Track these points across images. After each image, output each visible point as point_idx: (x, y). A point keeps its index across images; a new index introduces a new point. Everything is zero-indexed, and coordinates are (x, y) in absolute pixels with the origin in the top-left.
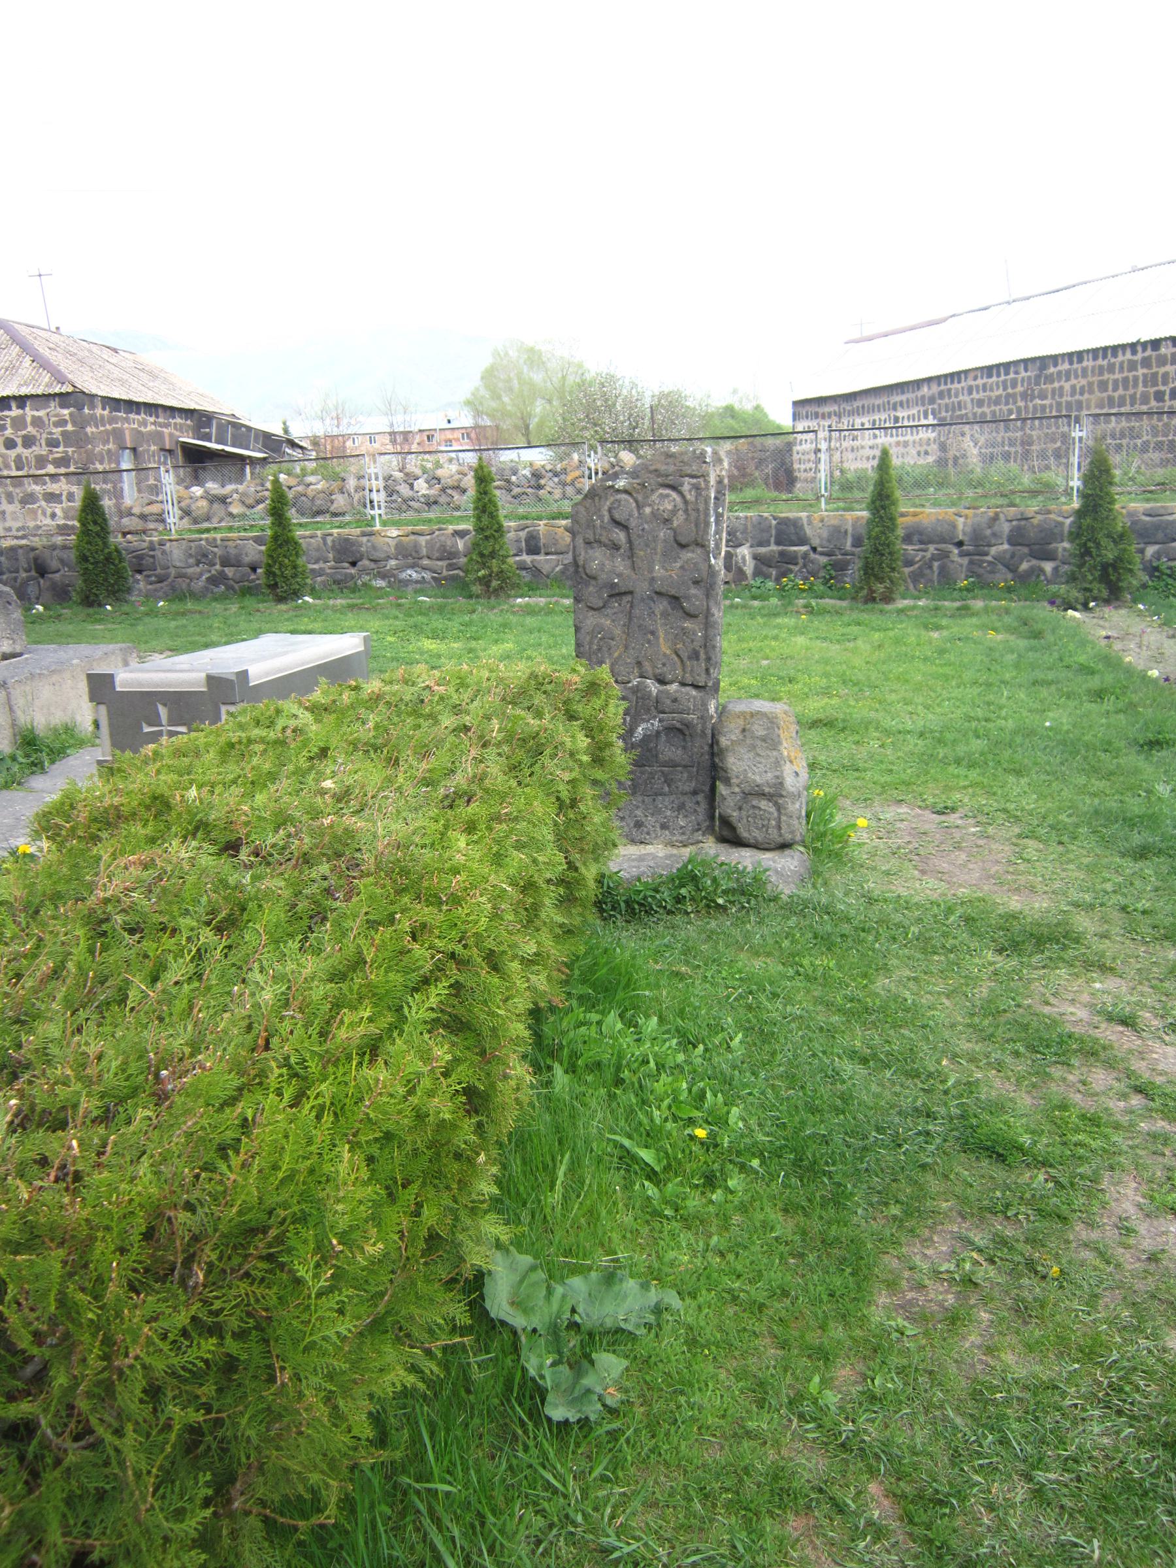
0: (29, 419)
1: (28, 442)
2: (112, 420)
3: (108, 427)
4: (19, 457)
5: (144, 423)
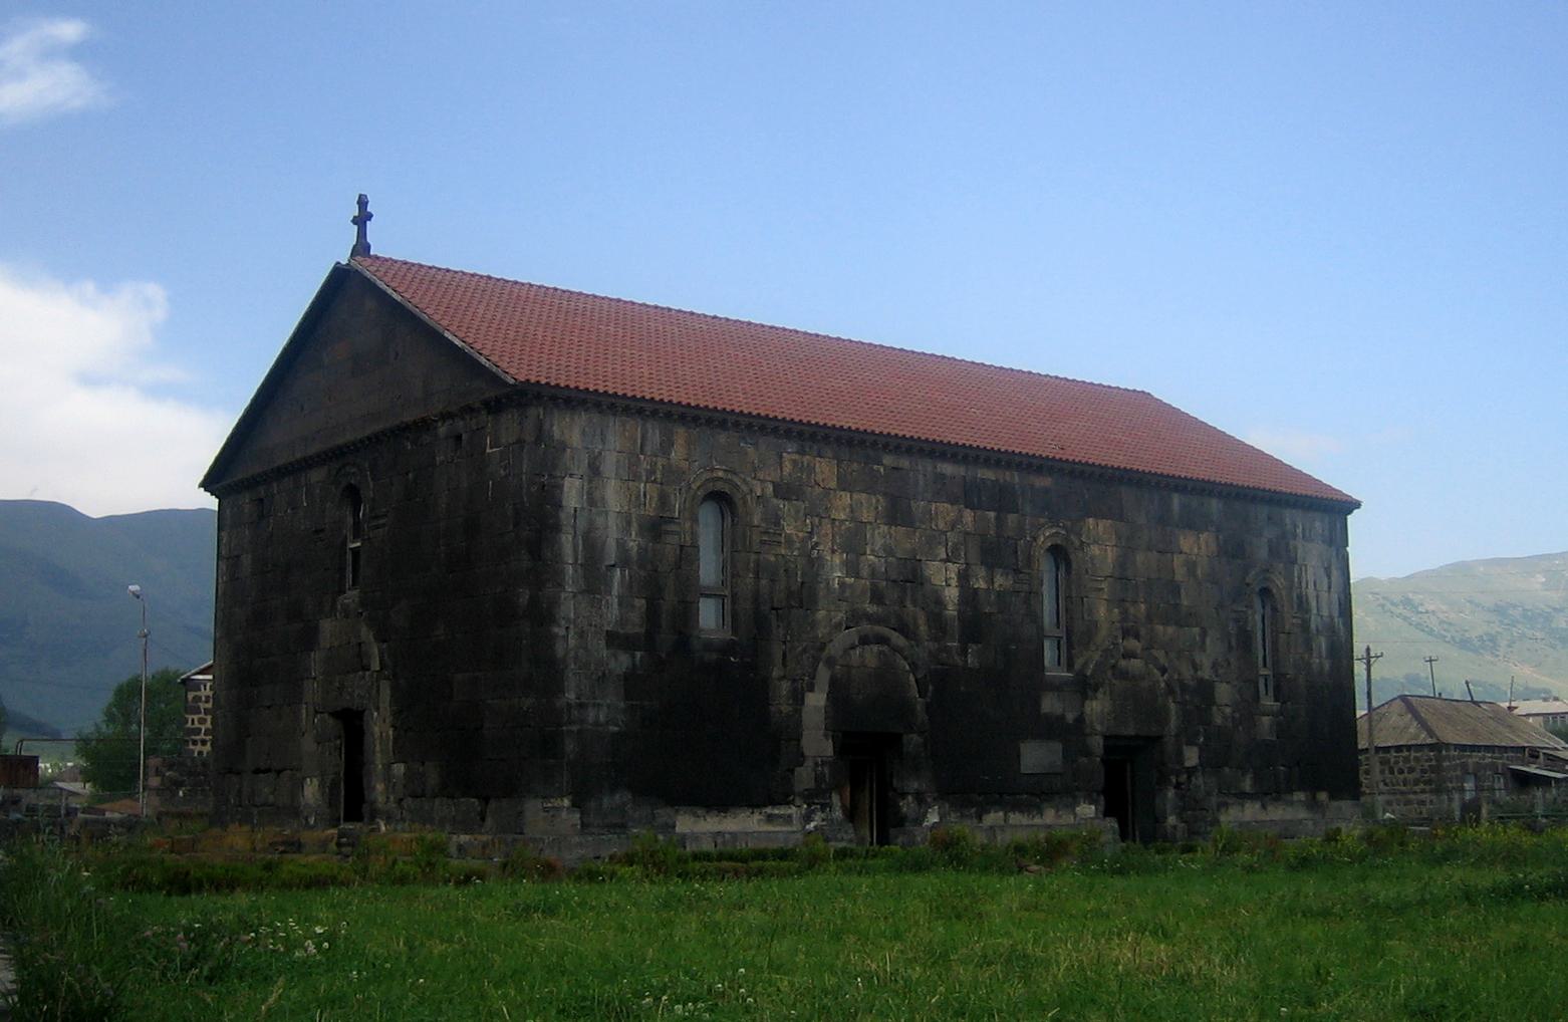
0: (1412, 757)
1: (1411, 770)
2: (1463, 757)
3: (1458, 762)
4: (1405, 779)
5: (1484, 758)
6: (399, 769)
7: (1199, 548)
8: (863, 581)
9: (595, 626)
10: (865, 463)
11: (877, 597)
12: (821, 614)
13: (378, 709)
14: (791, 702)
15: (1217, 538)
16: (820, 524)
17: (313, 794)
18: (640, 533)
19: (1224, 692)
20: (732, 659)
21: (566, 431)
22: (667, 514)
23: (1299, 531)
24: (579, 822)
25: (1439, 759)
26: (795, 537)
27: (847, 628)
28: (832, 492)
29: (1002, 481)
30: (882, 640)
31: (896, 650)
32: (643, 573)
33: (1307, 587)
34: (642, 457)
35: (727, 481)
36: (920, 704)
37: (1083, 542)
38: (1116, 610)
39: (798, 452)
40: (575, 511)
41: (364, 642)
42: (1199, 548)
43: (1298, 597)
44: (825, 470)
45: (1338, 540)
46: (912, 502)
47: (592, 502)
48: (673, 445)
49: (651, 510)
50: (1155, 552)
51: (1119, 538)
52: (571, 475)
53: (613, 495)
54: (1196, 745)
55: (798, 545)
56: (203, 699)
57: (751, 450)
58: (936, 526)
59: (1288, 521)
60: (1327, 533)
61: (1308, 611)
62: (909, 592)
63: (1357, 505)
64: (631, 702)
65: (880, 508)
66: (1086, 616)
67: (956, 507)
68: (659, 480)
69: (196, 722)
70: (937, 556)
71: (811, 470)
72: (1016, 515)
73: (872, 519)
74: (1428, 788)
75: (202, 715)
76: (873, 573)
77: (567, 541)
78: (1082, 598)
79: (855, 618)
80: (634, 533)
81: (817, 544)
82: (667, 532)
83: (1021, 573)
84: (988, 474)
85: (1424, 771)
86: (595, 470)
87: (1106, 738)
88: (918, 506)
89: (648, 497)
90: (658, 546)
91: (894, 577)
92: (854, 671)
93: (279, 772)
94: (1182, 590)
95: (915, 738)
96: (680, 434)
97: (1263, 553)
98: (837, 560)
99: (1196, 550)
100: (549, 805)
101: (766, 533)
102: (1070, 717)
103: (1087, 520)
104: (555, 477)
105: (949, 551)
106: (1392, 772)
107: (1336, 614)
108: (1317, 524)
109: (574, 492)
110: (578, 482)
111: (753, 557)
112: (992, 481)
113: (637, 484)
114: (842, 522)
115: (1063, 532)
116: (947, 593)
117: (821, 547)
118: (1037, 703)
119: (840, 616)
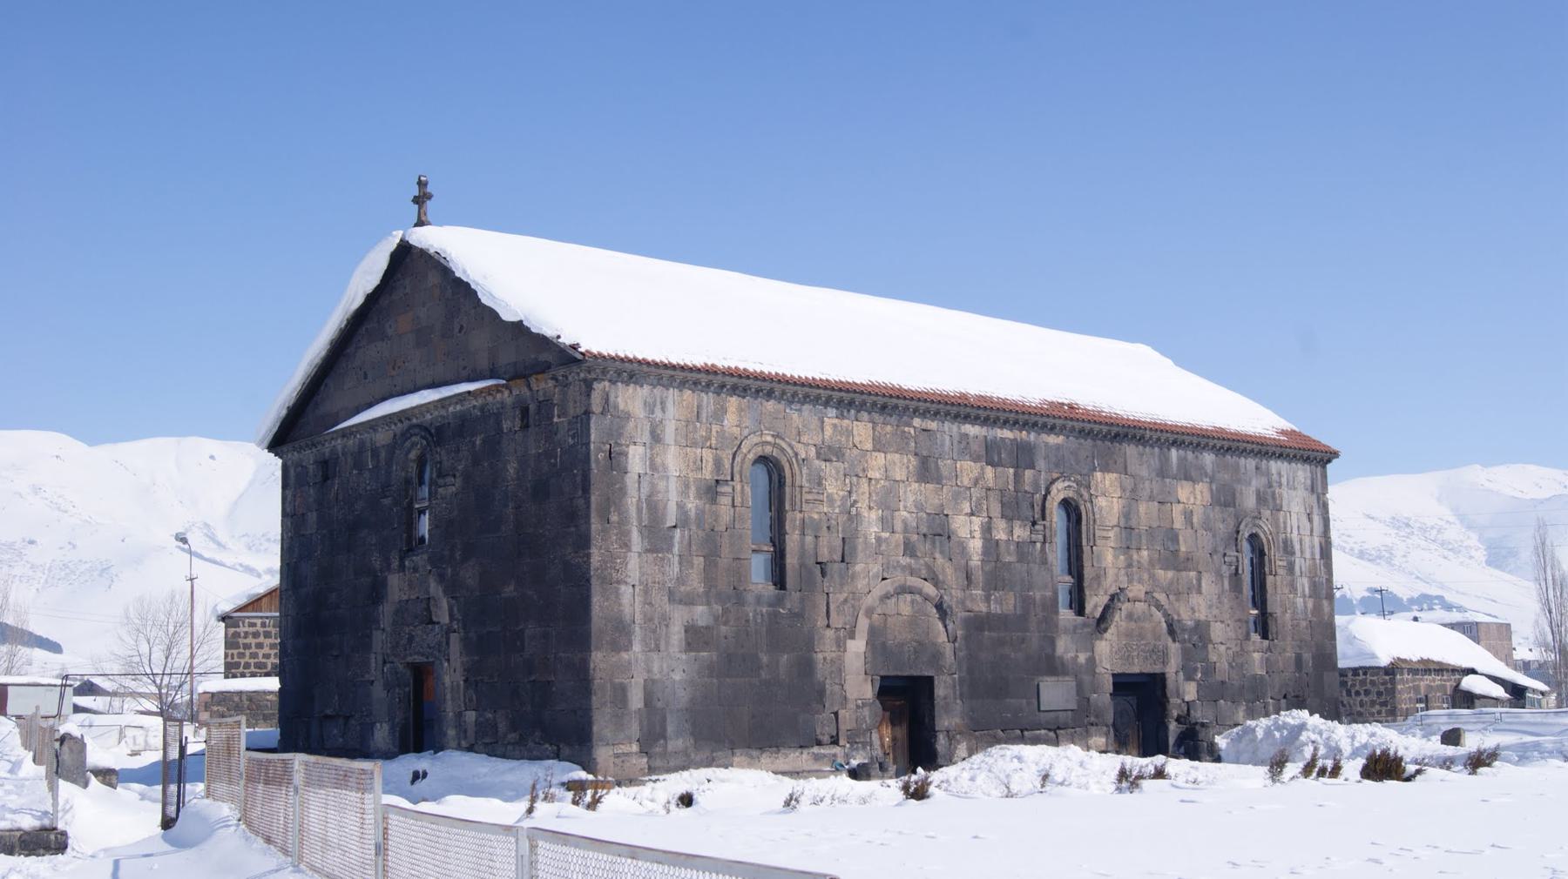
0: (1368, 681)
1: (1367, 693)
2: (1414, 681)
3: (1411, 685)
4: (1361, 700)
5: (1434, 681)
6: (471, 716)
7: (1195, 498)
9: (659, 583)
10: (897, 426)
12: (859, 567)
13: (448, 660)
15: (1211, 490)
16: (858, 483)
17: (384, 738)
19: (1218, 632)
20: (781, 610)
23: (1284, 480)
24: (647, 766)
25: (1393, 682)
26: (836, 496)
27: (883, 579)
29: (1019, 440)
30: (911, 591)
33: (1291, 532)
34: (698, 424)
35: (774, 445)
36: (948, 649)
37: (1091, 495)
38: (1122, 557)
39: (837, 417)
40: (640, 477)
41: (433, 598)
42: (1195, 498)
43: (1283, 543)
44: (862, 430)
45: (1318, 489)
47: (653, 467)
49: (708, 474)
50: (1156, 504)
51: (1123, 490)
52: (635, 443)
53: (673, 460)
54: (1194, 680)
55: (839, 503)
56: (242, 635)
57: (795, 416)
58: (961, 482)
59: (1274, 471)
60: (1309, 482)
61: (1293, 553)
62: (938, 544)
63: (1335, 454)
64: (693, 654)
65: (911, 467)
66: (1095, 564)
68: (713, 446)
69: (235, 657)
70: (962, 510)
71: (849, 433)
72: (1032, 471)
74: (1384, 709)
75: (241, 650)
76: (906, 530)
77: (631, 502)
78: (1092, 547)
81: (855, 502)
82: (723, 494)
84: (1007, 434)
85: (1379, 694)
86: (656, 438)
87: (1114, 675)
88: (945, 465)
89: (704, 461)
91: (924, 530)
92: (889, 619)
93: (347, 718)
94: (1181, 538)
96: (733, 402)
97: (1250, 501)
98: (874, 515)
99: (1192, 500)
100: (620, 751)
102: (1082, 658)
105: (973, 504)
106: (1349, 693)
107: (1318, 556)
108: (1300, 473)
109: (637, 457)
111: (799, 516)
113: (694, 449)
114: (877, 481)
115: (1075, 485)
117: (859, 505)
119: (876, 568)
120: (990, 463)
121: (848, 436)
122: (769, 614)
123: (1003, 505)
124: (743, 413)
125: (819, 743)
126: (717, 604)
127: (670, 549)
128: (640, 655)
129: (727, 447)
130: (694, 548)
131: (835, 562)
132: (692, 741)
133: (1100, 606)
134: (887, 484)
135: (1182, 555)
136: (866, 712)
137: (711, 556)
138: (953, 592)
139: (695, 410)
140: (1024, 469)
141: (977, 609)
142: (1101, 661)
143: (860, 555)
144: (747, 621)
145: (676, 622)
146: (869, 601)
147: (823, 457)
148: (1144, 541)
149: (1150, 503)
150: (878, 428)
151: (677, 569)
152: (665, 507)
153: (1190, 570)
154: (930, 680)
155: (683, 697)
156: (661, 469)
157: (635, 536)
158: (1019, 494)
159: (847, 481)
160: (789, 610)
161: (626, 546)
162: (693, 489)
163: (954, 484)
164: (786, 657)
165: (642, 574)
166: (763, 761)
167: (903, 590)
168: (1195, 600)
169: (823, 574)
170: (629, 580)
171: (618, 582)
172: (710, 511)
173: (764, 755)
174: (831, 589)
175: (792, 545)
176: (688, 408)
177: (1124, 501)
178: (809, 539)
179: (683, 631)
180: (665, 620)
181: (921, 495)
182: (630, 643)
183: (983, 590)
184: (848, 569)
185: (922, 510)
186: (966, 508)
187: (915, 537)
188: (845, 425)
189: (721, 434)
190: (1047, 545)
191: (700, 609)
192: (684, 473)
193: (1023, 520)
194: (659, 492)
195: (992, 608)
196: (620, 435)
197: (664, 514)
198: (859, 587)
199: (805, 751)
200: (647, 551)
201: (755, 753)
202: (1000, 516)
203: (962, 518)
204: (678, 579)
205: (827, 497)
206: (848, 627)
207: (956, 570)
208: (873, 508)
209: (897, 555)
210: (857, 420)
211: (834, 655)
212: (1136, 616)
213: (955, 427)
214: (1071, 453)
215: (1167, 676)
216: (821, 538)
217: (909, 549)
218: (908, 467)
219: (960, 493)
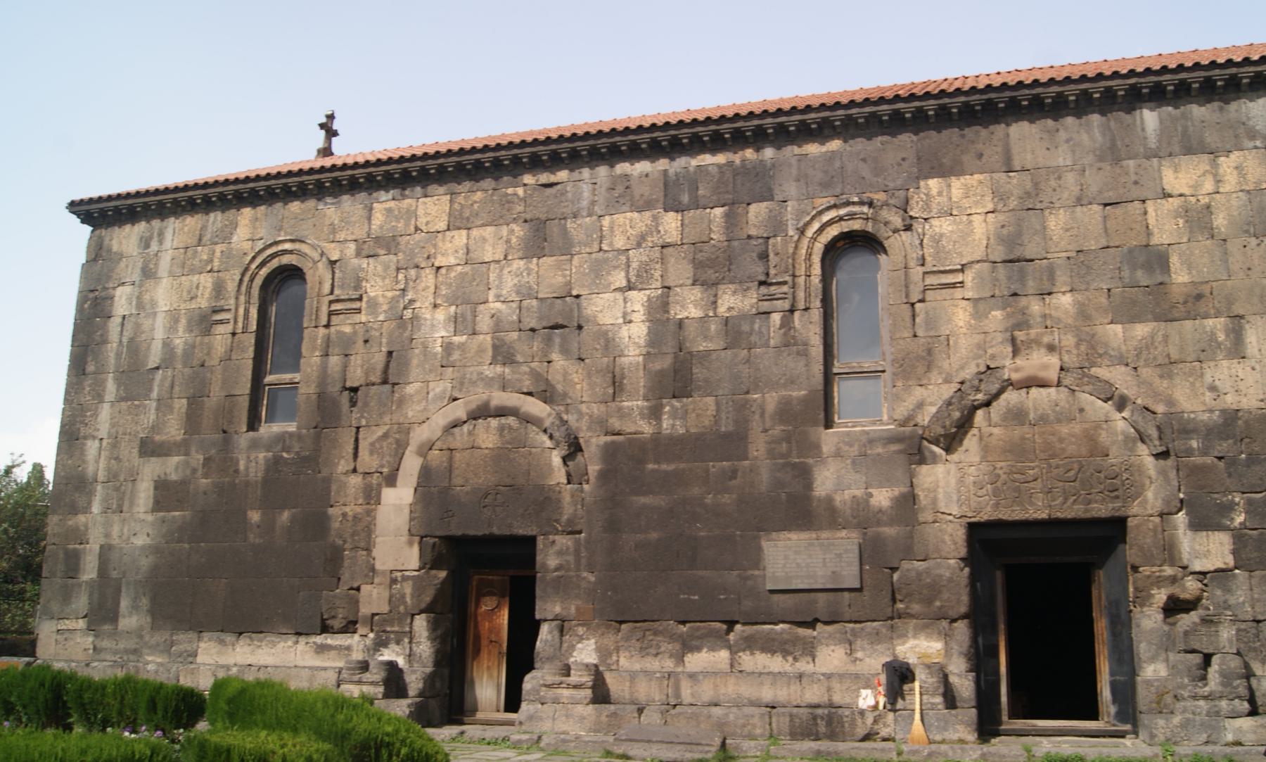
8: (481, 337)
11: (502, 354)
12: (410, 389)
14: (360, 501)
18: (189, 329)
20: (285, 455)
21: (124, 242)
22: (222, 303)
24: (91, 647)
26: (381, 300)
27: (455, 399)
28: (439, 235)
30: (501, 412)
31: (528, 420)
32: (187, 371)
38: (997, 314)
46: (569, 224)
47: (140, 306)
48: (235, 229)
49: (203, 302)
51: (999, 195)
53: (164, 295)
55: (385, 307)
58: (611, 244)
62: (557, 340)
64: (162, 514)
65: (514, 240)
66: (920, 333)
67: (647, 214)
68: (215, 269)
71: (412, 214)
72: (765, 204)
73: (499, 256)
76: (498, 326)
77: (112, 348)
78: (913, 305)
79: (461, 383)
80: (181, 330)
81: (412, 301)
83: (771, 284)
86: (148, 273)
89: (201, 288)
90: (206, 339)
91: (533, 324)
92: (457, 456)
94: (1174, 260)
95: (563, 541)
98: (440, 315)
99: (1209, 186)
100: (64, 627)
101: (338, 301)
102: (882, 498)
103: (922, 183)
104: (108, 289)
105: (632, 273)
109: (123, 301)
110: (127, 289)
111: (322, 331)
112: (719, 166)
113: (190, 277)
114: (449, 267)
116: (624, 332)
117: (417, 305)
118: (805, 475)
119: (440, 387)
120: (673, 205)
121: (409, 219)
122: (267, 460)
123: (698, 265)
124: (258, 223)
125: (325, 629)
126: (197, 452)
127: (147, 397)
128: (99, 518)
129: (233, 266)
130: (177, 389)
131: (373, 384)
132: (149, 619)
133: (931, 404)
134: (468, 268)
135: (1177, 293)
136: (408, 589)
137: (195, 402)
138: (584, 408)
139: (198, 232)
140: (749, 204)
141: (632, 429)
142: (934, 501)
143: (415, 372)
144: (237, 471)
145: (145, 478)
146: (420, 435)
147: (365, 253)
148: (1062, 279)
149: (1079, 209)
150: (461, 199)
151: (153, 417)
152: (148, 348)
153: (1206, 317)
154: (531, 541)
155: (145, 563)
156: (148, 306)
157: (111, 387)
158: (736, 244)
159: (401, 276)
160: (297, 453)
161: (100, 398)
162: (183, 321)
163: (596, 247)
164: (286, 515)
165: (113, 425)
166: (238, 650)
167: (481, 413)
168: (1222, 372)
169: (353, 403)
170: (96, 434)
171: (85, 438)
172: (201, 344)
173: (241, 642)
174: (364, 422)
175: (309, 370)
176: (189, 232)
177: (1001, 217)
178: (335, 361)
179: (152, 488)
180: (132, 476)
181: (529, 274)
182: (90, 503)
183: (646, 399)
184: (393, 392)
185: (530, 296)
186: (619, 279)
187: (515, 335)
188: (405, 206)
189: (227, 255)
190: (797, 314)
191: (176, 459)
192: (175, 306)
193: (740, 282)
194: (143, 332)
195: (665, 426)
196: (109, 278)
197: (146, 356)
198: (410, 414)
199: (302, 640)
200: (122, 399)
201: (229, 638)
202: (690, 282)
203: (606, 296)
204: (153, 427)
205: (368, 302)
206: (385, 470)
207: (589, 375)
208: (440, 305)
209: (480, 364)
210: (426, 196)
211: (359, 509)
212: (1032, 416)
213: (602, 171)
214: (864, 160)
215: (1131, 523)
216: (352, 358)
217: (502, 354)
218: (508, 241)
219: (606, 260)
